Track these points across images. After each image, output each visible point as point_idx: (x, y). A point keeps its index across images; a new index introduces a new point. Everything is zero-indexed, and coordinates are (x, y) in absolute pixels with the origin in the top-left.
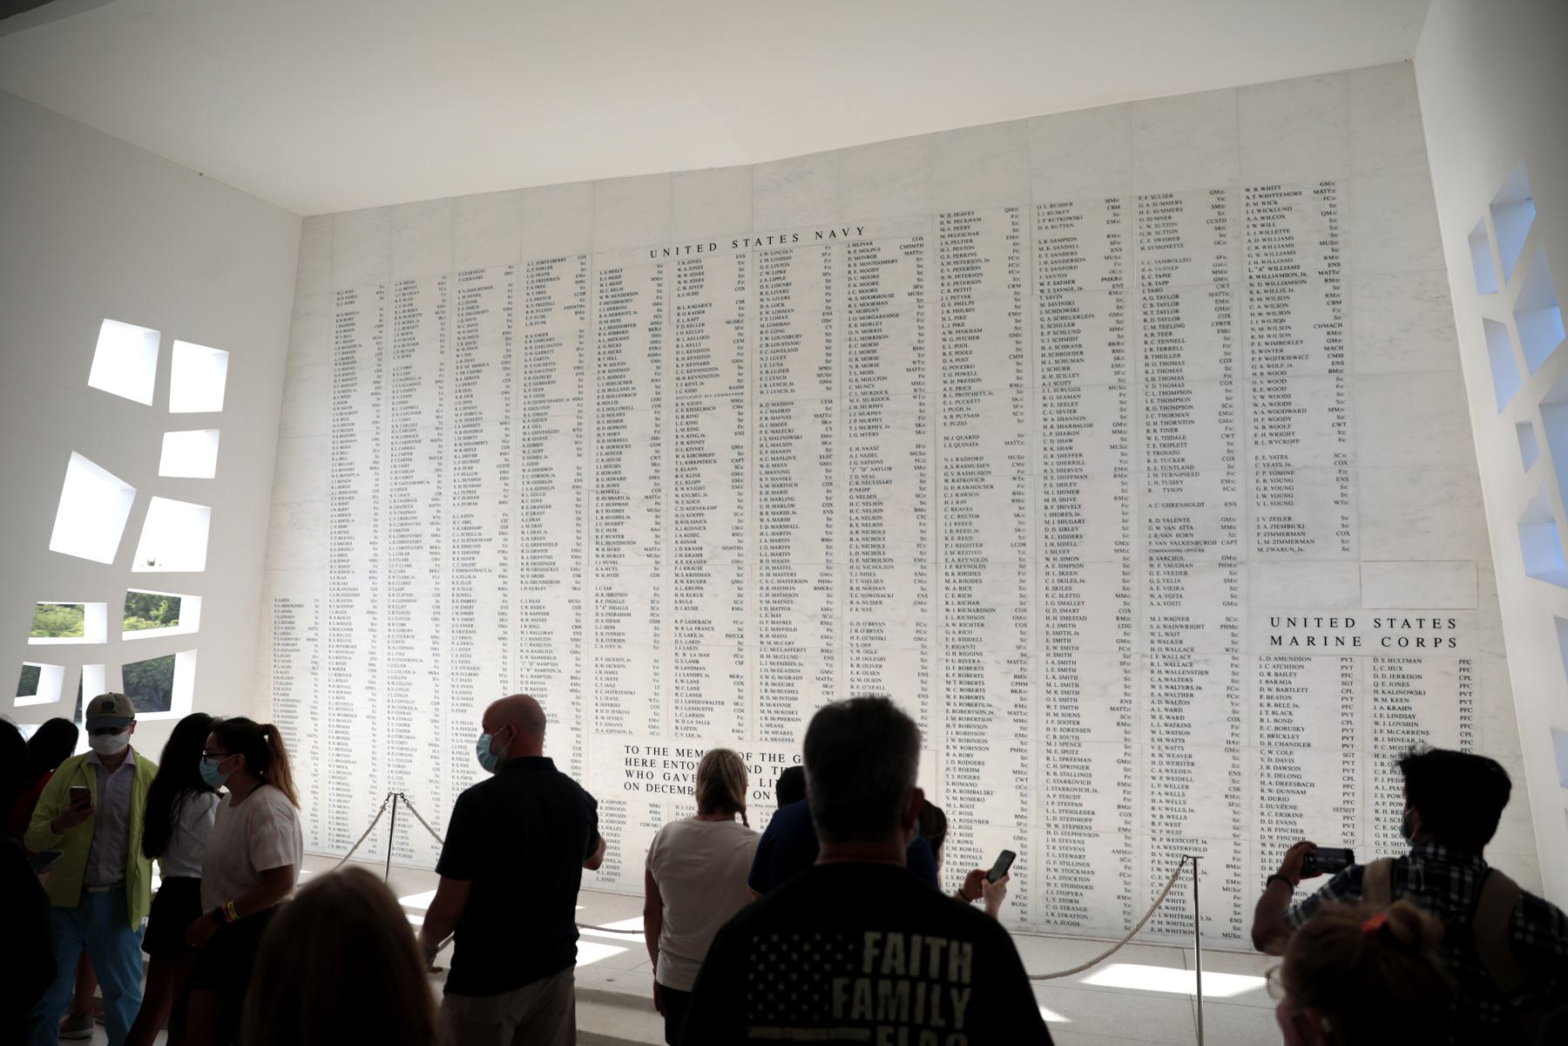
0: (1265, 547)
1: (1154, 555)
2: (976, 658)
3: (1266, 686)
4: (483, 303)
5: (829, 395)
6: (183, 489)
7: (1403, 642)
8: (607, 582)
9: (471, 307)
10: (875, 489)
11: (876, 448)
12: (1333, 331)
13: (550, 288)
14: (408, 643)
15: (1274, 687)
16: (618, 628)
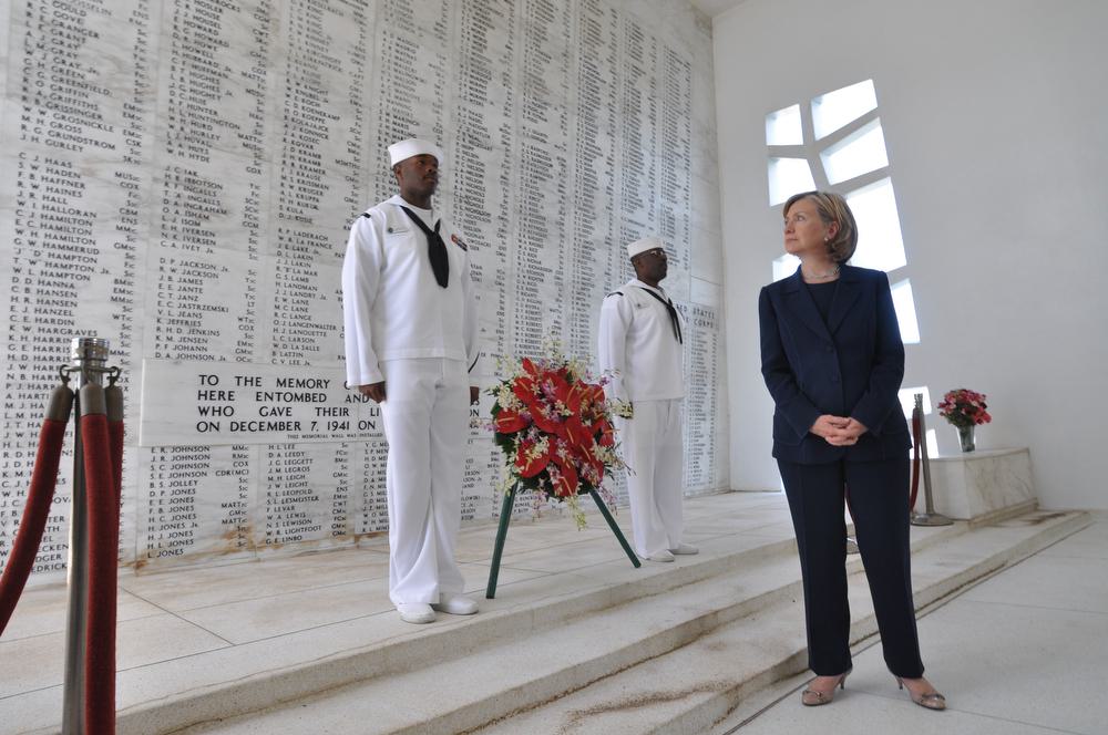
2: (537, 305)
8: (187, 164)
10: (477, 151)
16: (204, 226)
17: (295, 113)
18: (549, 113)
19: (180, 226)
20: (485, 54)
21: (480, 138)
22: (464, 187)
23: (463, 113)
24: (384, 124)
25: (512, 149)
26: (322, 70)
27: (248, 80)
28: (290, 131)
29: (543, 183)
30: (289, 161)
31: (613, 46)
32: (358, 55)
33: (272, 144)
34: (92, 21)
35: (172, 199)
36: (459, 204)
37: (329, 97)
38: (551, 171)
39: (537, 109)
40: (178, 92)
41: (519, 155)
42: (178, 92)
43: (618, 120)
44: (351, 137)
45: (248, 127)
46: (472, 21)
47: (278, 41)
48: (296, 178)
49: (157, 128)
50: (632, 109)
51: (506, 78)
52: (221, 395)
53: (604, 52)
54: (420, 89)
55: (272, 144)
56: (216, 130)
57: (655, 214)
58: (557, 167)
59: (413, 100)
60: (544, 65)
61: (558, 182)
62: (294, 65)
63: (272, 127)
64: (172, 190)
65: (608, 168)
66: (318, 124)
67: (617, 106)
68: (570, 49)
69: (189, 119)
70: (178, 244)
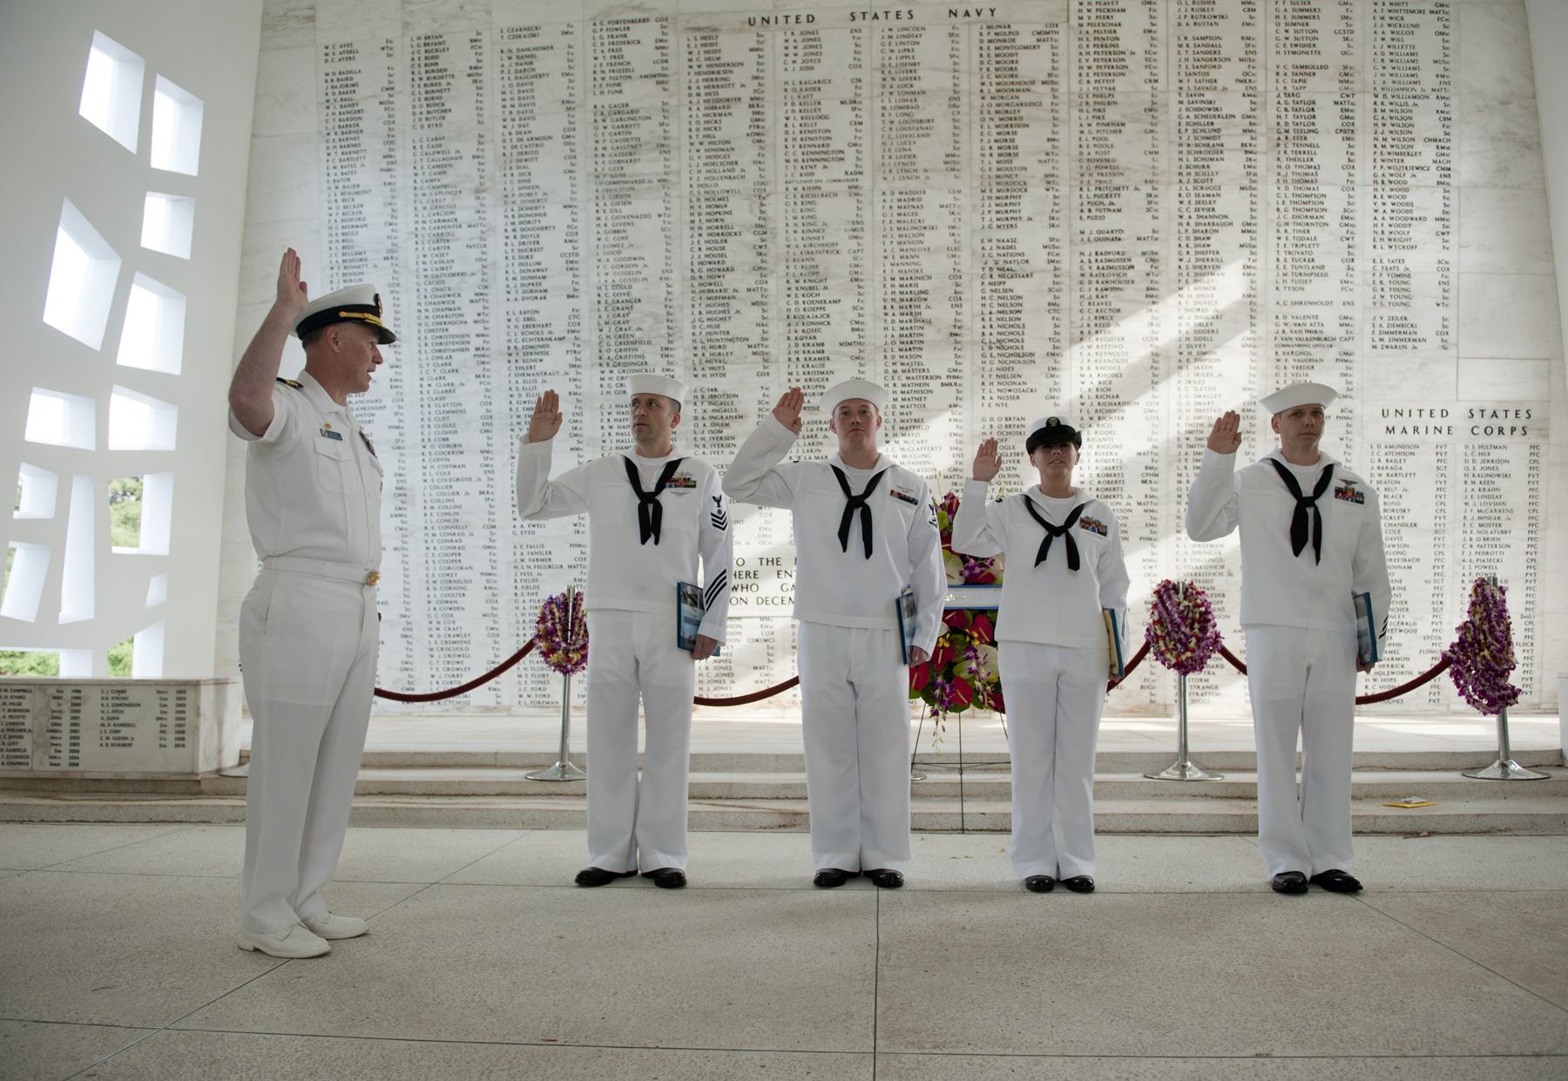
0: (1379, 344)
1: (1280, 351)
3: (1376, 472)
4: (539, 67)
5: (958, 184)
6: (159, 267)
7: (1488, 431)
8: (709, 383)
9: (524, 66)
10: (1010, 283)
11: (1014, 241)
12: (1441, 144)
13: (628, 52)
14: (455, 459)
15: (1384, 472)
16: (726, 432)
17: (797, 310)
18: (1131, 200)
19: (707, 436)
20: (1017, 163)
21: (1014, 266)
22: (994, 331)
23: (987, 245)
24: (889, 290)
25: (1064, 266)
26: (818, 257)
27: (752, 294)
28: (793, 328)
29: (1118, 293)
30: (794, 357)
31: (1249, 57)
32: (856, 228)
33: (778, 347)
34: (635, 294)
35: (700, 415)
36: (988, 353)
37: (829, 283)
38: (1131, 274)
39: (1103, 199)
40: (698, 324)
41: (1076, 270)
42: (698, 324)
43: (1264, 162)
44: (854, 316)
45: (755, 336)
46: (994, 131)
47: (776, 248)
48: (801, 370)
49: (686, 359)
50: (1297, 135)
51: (1050, 180)
52: (748, 574)
53: (1226, 75)
54: (930, 238)
55: (778, 347)
56: (728, 344)
57: (1358, 278)
58: (1141, 265)
59: (922, 254)
60: (1112, 138)
61: (1144, 286)
62: (791, 264)
63: (777, 330)
64: (700, 408)
65: (1246, 238)
66: (819, 313)
67: (1261, 143)
68: (1160, 98)
69: (707, 345)
70: (707, 451)
